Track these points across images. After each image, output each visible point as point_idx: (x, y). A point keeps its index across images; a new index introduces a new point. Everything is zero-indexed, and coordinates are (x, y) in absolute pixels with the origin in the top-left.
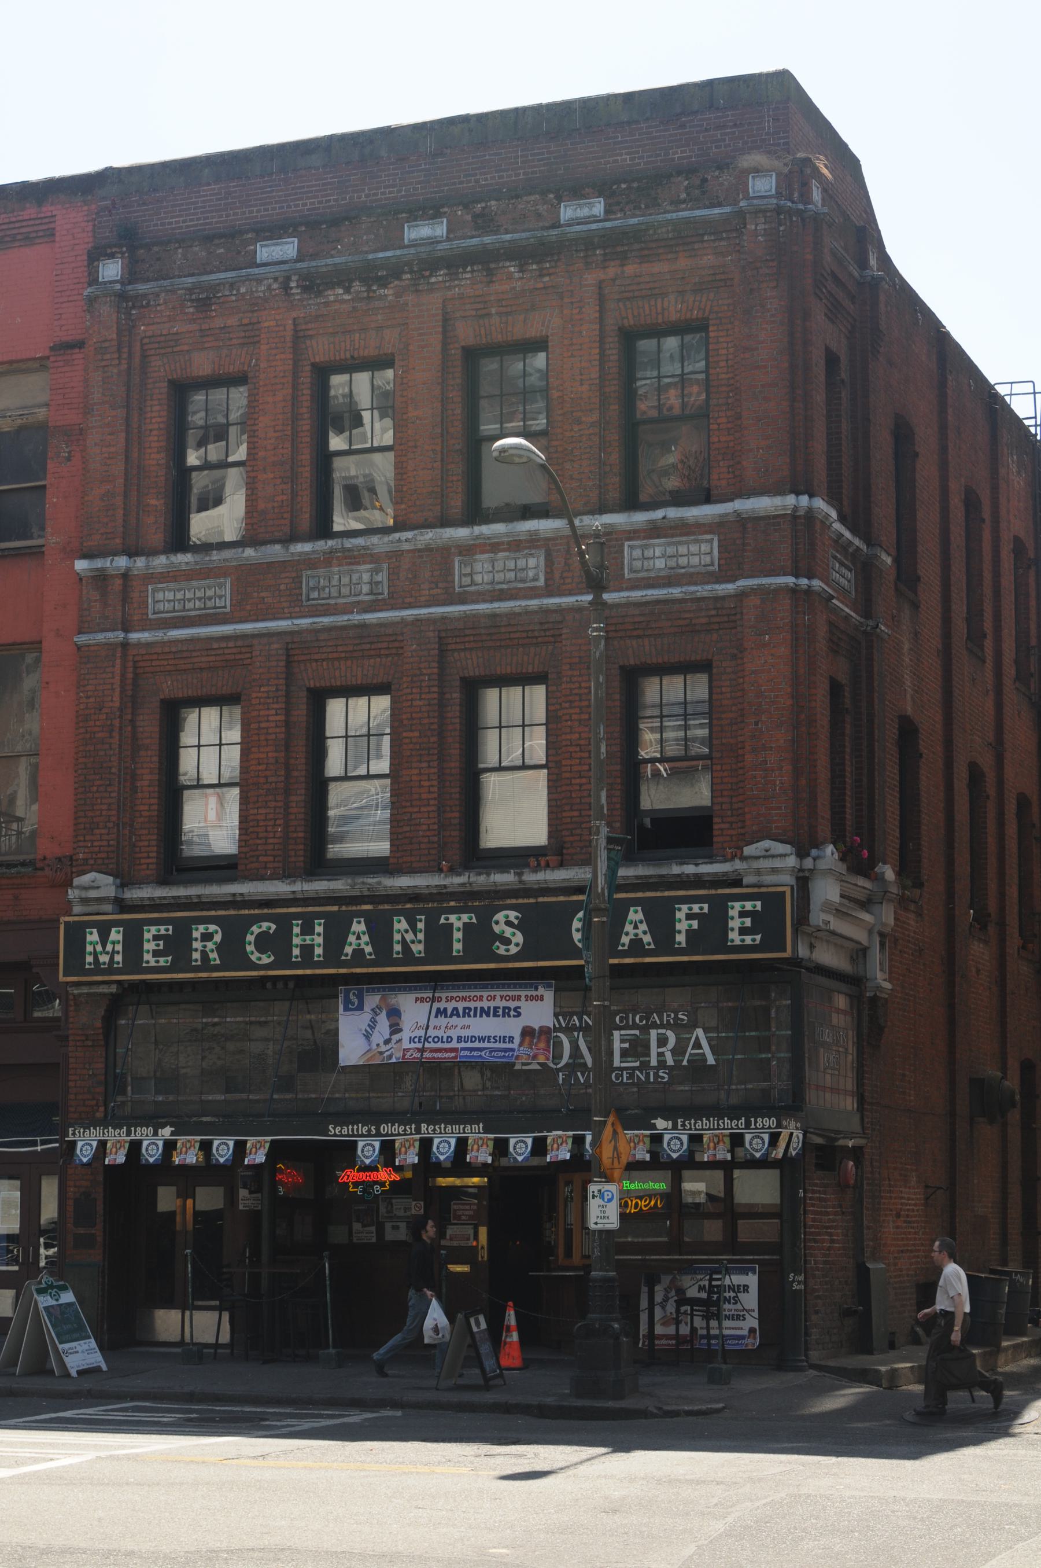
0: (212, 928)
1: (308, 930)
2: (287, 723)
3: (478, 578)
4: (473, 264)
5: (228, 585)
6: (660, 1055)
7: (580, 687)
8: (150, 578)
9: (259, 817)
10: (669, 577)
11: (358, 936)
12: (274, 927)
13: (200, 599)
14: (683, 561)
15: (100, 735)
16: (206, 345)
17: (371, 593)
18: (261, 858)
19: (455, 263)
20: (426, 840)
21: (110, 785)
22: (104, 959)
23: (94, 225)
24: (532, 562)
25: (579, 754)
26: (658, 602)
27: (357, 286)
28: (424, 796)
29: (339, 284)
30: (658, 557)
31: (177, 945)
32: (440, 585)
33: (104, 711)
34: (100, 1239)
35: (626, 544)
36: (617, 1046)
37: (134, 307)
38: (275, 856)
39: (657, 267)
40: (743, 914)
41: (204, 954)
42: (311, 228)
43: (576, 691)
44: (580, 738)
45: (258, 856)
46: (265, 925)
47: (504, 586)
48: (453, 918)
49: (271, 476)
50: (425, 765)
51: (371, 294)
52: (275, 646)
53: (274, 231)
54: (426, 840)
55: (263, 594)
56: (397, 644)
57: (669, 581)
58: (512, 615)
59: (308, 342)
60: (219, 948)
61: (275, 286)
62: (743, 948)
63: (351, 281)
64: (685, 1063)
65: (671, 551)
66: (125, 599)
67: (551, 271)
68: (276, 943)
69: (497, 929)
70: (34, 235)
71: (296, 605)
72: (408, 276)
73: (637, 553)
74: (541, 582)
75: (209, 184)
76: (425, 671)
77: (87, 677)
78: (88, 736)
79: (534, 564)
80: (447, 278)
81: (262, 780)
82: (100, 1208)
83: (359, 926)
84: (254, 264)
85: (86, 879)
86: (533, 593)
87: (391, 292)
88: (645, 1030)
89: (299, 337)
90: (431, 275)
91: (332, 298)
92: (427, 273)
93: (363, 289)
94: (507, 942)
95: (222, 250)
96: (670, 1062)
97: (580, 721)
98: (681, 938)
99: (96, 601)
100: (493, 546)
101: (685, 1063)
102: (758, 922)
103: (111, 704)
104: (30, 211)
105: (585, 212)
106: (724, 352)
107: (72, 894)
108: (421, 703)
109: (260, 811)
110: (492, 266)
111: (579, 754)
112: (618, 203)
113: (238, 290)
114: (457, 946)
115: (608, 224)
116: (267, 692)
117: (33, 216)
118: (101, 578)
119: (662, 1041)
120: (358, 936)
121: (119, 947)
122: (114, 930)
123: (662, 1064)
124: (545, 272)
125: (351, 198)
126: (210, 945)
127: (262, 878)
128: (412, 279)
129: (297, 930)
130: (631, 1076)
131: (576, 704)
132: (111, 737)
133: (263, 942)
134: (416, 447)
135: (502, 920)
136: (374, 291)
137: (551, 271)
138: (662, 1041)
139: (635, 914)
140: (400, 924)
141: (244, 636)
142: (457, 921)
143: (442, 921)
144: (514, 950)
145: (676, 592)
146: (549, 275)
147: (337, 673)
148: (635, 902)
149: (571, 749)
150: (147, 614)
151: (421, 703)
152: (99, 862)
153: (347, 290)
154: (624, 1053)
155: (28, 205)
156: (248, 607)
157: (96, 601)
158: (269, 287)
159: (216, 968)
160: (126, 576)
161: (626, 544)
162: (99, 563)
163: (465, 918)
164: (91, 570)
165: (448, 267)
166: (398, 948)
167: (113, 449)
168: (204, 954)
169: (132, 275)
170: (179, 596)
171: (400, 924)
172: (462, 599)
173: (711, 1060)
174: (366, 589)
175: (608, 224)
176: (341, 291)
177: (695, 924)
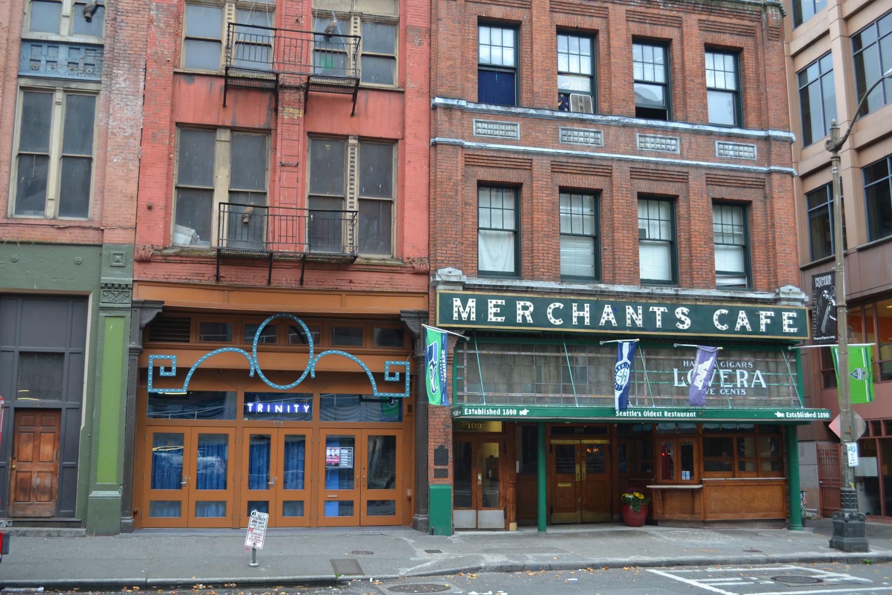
0: (528, 304)
1: (581, 308)
6: (742, 382)
12: (562, 306)
14: (741, 153)
22: (464, 316)
24: (673, 142)
26: (732, 170)
31: (508, 310)
34: (451, 472)
35: (717, 142)
36: (722, 377)
40: (789, 318)
41: (524, 317)
46: (558, 305)
48: (656, 309)
58: (665, 164)
60: (532, 314)
62: (790, 334)
65: (736, 148)
68: (564, 314)
69: (678, 316)
71: (556, 142)
74: (678, 152)
82: (450, 455)
83: (608, 309)
85: (446, 270)
86: (675, 156)
88: (734, 370)
94: (683, 323)
96: (746, 385)
98: (763, 328)
102: (796, 322)
114: (659, 324)
119: (742, 376)
121: (474, 310)
122: (470, 300)
123: (743, 386)
126: (527, 313)
127: (542, 280)
129: (575, 308)
130: (729, 392)
133: (556, 313)
135: (680, 312)
138: (742, 376)
139: (742, 314)
140: (630, 310)
142: (659, 311)
143: (651, 310)
144: (686, 327)
148: (742, 308)
154: (726, 380)
161: (717, 142)
163: (662, 309)
164: (445, 104)
166: (629, 322)
168: (524, 317)
170: (491, 126)
171: (630, 310)
173: (764, 386)
177: (769, 321)
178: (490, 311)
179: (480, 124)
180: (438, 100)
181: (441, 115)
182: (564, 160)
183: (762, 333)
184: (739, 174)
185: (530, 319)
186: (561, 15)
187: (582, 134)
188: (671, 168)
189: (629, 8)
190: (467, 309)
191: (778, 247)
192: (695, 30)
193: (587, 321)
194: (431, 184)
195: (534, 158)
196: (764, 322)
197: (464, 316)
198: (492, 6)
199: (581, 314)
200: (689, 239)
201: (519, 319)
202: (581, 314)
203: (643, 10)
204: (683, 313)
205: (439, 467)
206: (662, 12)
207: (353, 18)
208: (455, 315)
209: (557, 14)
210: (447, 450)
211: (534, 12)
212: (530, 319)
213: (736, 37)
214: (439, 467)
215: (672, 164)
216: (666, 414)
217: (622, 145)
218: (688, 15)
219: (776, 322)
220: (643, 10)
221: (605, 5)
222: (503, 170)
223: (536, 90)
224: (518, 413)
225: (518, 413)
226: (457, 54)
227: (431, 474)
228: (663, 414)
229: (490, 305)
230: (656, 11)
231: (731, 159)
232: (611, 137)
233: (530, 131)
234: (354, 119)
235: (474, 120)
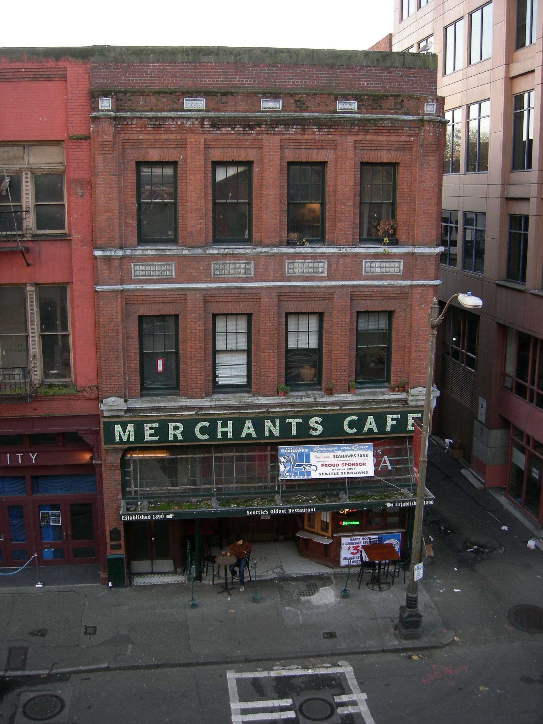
0: (178, 424)
1: (225, 425)
3: (296, 270)
4: (296, 125)
5: (173, 265)
7: (342, 321)
9: (192, 372)
10: (381, 276)
11: (249, 428)
13: (159, 271)
14: (387, 269)
15: (112, 334)
16: (156, 146)
17: (245, 274)
18: (194, 390)
19: (287, 123)
20: (272, 383)
21: (118, 357)
22: (125, 439)
23: (90, 76)
24: (321, 265)
25: (341, 349)
28: (271, 365)
29: (230, 125)
30: (377, 267)
32: (279, 272)
33: (113, 323)
34: (123, 545)
37: (119, 124)
38: (201, 389)
39: (381, 138)
41: (175, 435)
43: (340, 322)
44: (341, 342)
45: (192, 389)
47: (308, 275)
48: (291, 420)
49: (195, 215)
50: (271, 351)
51: (245, 132)
52: (198, 295)
53: (193, 94)
54: (272, 383)
55: (191, 271)
56: (257, 297)
57: (382, 278)
58: (312, 287)
59: (210, 150)
61: (196, 123)
63: (236, 125)
64: (379, 469)
65: (382, 265)
67: (333, 133)
68: (211, 430)
70: (53, 76)
71: (208, 277)
72: (265, 126)
73: (368, 264)
74: (325, 274)
75: (153, 63)
76: (271, 311)
77: (103, 306)
78: (105, 334)
79: (322, 267)
80: (284, 130)
81: (194, 356)
82: (122, 534)
83: (249, 423)
84: (183, 110)
86: (322, 279)
87: (255, 132)
90: (276, 128)
91: (225, 132)
92: (275, 126)
93: (241, 129)
94: (316, 430)
95: (165, 100)
97: (341, 335)
98: (388, 429)
99: (105, 270)
100: (304, 256)
101: (379, 469)
103: (116, 320)
104: (51, 64)
105: (347, 106)
106: (407, 179)
108: (270, 324)
109: (193, 369)
110: (306, 127)
111: (341, 349)
112: (364, 105)
113: (177, 122)
114: (294, 433)
115: (358, 116)
116: (195, 316)
117: (53, 67)
120: (249, 428)
121: (132, 433)
122: (129, 425)
124: (330, 133)
125: (230, 81)
126: (178, 432)
128: (266, 128)
131: (340, 328)
132: (117, 335)
133: (203, 430)
134: (267, 208)
136: (247, 131)
137: (333, 133)
140: (268, 424)
145: (385, 282)
146: (332, 134)
147: (227, 308)
149: (337, 347)
150: (131, 277)
151: (270, 324)
152: (115, 391)
153: (233, 129)
155: (50, 60)
156: (184, 277)
157: (105, 270)
158: (193, 124)
161: (364, 261)
165: (285, 125)
167: (111, 196)
168: (175, 435)
170: (148, 268)
172: (289, 279)
173: (390, 468)
174: (243, 271)
175: (358, 116)
176: (230, 129)
177: (394, 423)
178: (146, 433)
179: (138, 268)
180: (98, 253)
181: (102, 266)
182: (216, 292)
183: (388, 433)
184: (384, 289)
185: (180, 437)
186: (217, 150)
187: (232, 266)
188: (318, 290)
189: (283, 137)
190: (127, 433)
191: (413, 354)
192: (350, 153)
193: (230, 435)
194: (97, 325)
195: (188, 293)
196: (390, 423)
197: (125, 439)
198: (150, 150)
199: (225, 429)
200: (331, 351)
201: (171, 438)
202: (225, 429)
203: (299, 137)
204: (317, 422)
205: (114, 543)
206: (317, 137)
207: (24, 173)
208: (117, 439)
209: (213, 150)
210: (120, 531)
211: (189, 152)
212: (180, 437)
213: (393, 153)
214: (114, 543)
215: (319, 287)
216: (290, 511)
217: (272, 272)
218: (344, 137)
219: (401, 423)
220: (299, 137)
221: (260, 137)
222: (160, 305)
223: (190, 229)
224: (165, 517)
225: (165, 517)
226: (115, 206)
227: (109, 547)
228: (287, 511)
229: (146, 428)
230: (311, 137)
231: (377, 276)
232: (261, 267)
233: (184, 268)
234: (29, 269)
235: (132, 264)
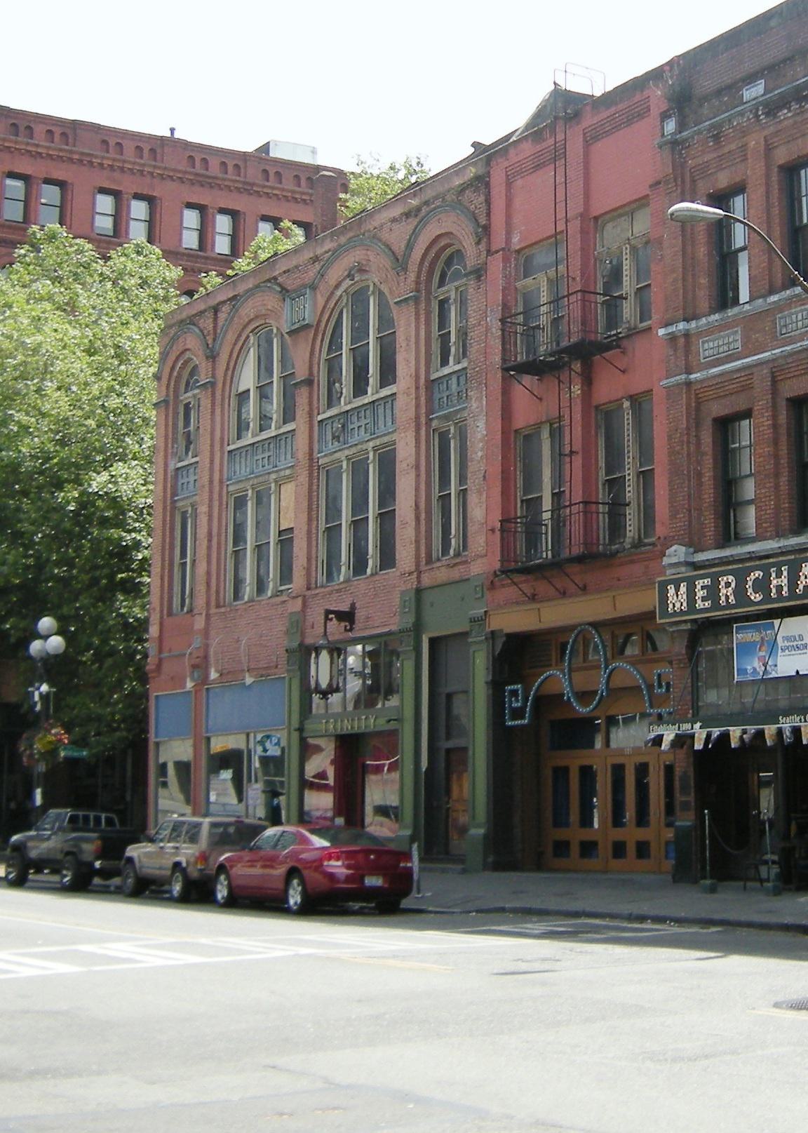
0: (731, 578)
1: (779, 575)
2: (775, 426)
8: (700, 334)
27: (795, 106)
31: (713, 592)
42: (770, 71)
66: (687, 350)
71: (776, 339)
89: (769, 149)
107: (666, 561)
118: (673, 338)
141: (749, 367)
153: (790, 111)
159: (734, 607)
160: (687, 335)
162: (672, 329)
169: (682, 126)
229: (699, 587)
